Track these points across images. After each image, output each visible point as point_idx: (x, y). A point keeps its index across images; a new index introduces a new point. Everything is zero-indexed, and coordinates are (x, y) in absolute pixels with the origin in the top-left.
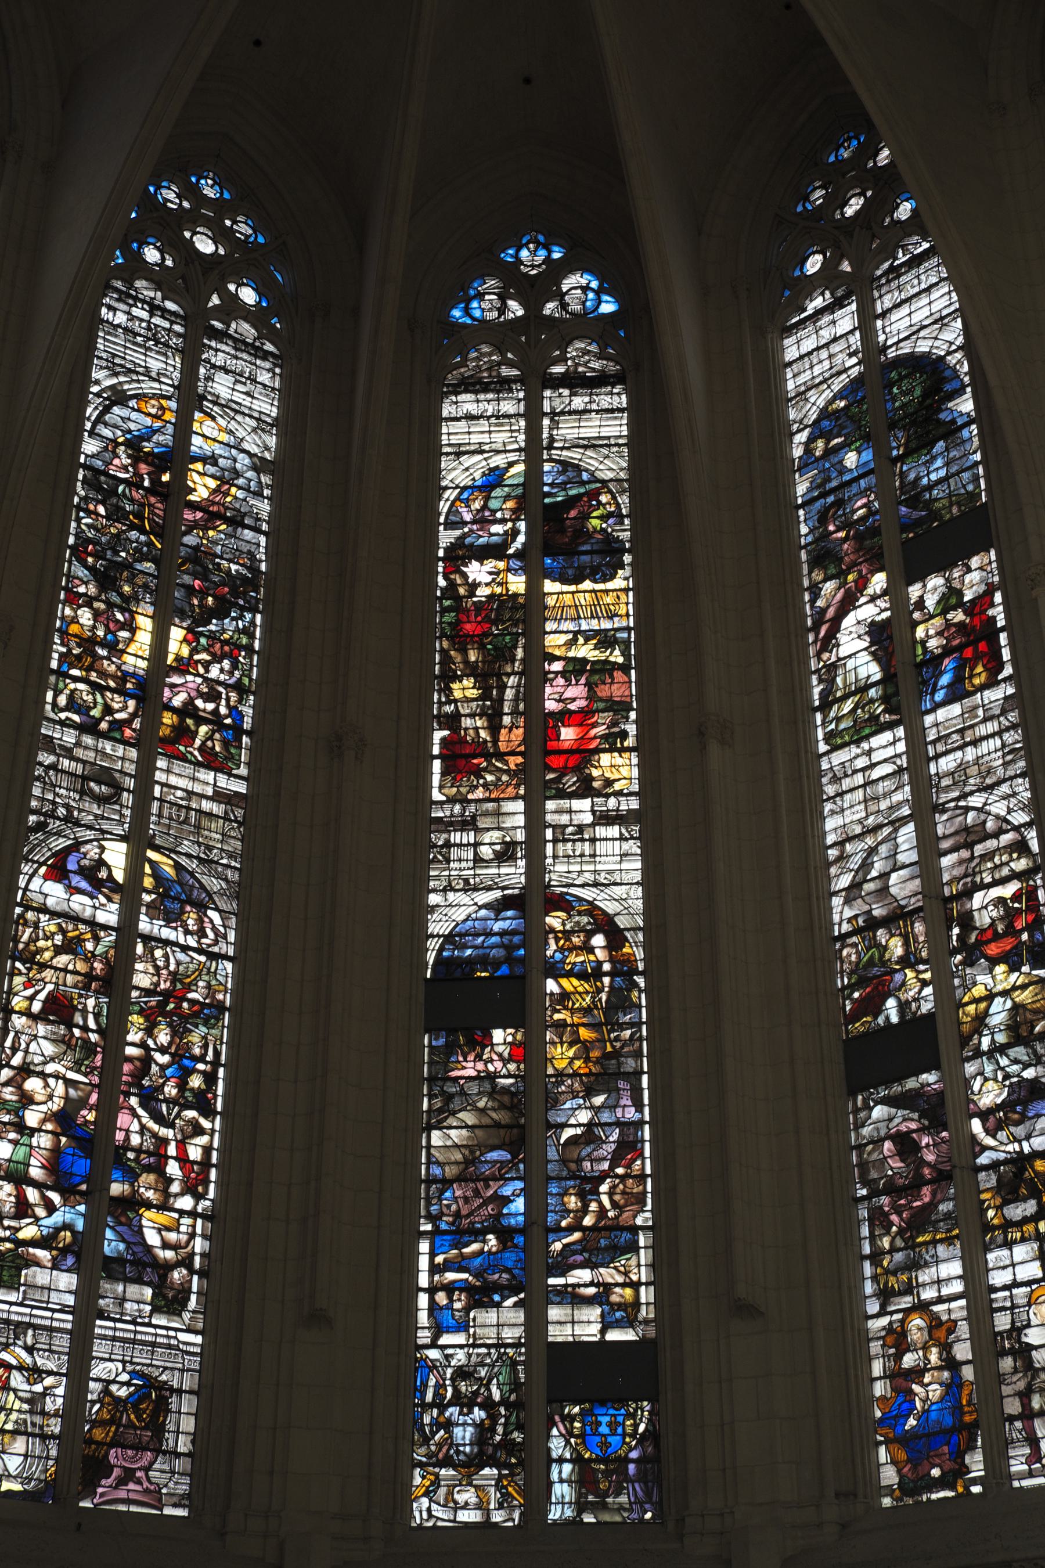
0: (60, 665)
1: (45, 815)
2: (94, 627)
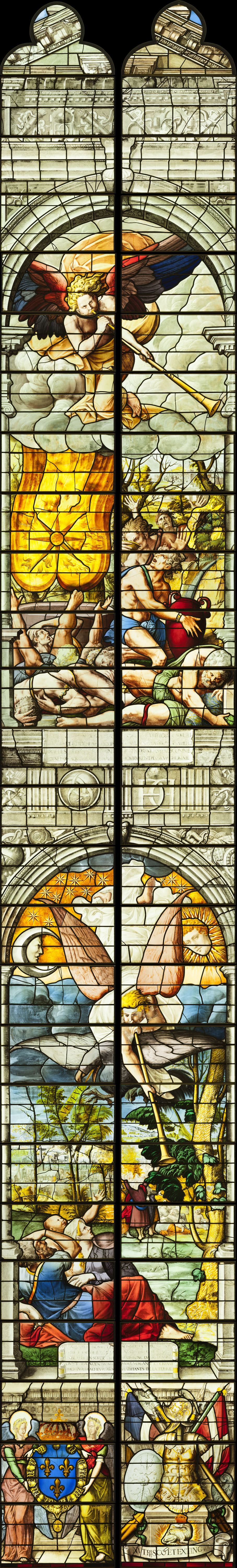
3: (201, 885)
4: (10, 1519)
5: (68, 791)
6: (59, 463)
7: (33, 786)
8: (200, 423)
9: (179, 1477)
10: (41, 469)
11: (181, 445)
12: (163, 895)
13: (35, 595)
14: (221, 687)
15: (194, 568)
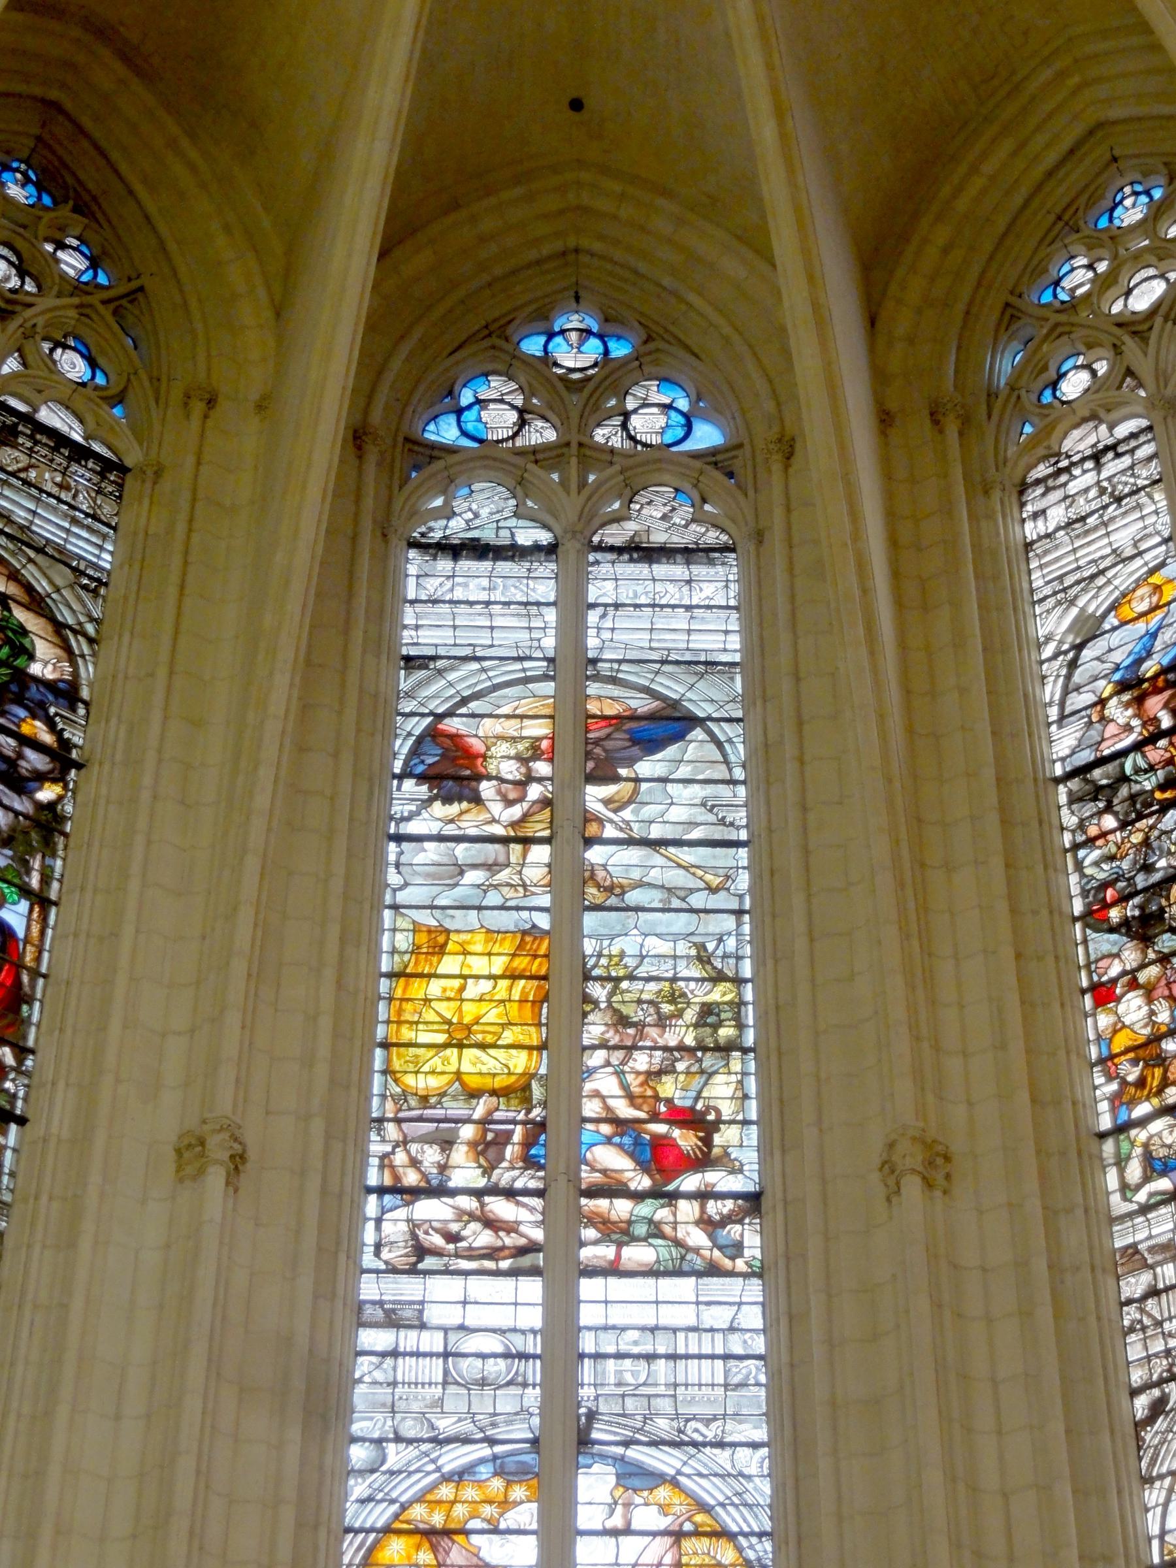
0: (1115, 1117)
1: (1161, 1382)
2: (1152, 1013)
3: (712, 1502)
5: (464, 1364)
6: (469, 943)
7: (405, 1354)
8: (698, 900)
10: (440, 950)
11: (669, 924)
12: (647, 1517)
13: (424, 1100)
14: (740, 1222)
15: (694, 1069)
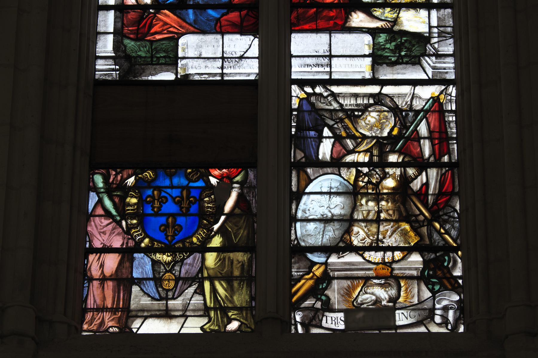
4: (95, 272)
9: (379, 212)
